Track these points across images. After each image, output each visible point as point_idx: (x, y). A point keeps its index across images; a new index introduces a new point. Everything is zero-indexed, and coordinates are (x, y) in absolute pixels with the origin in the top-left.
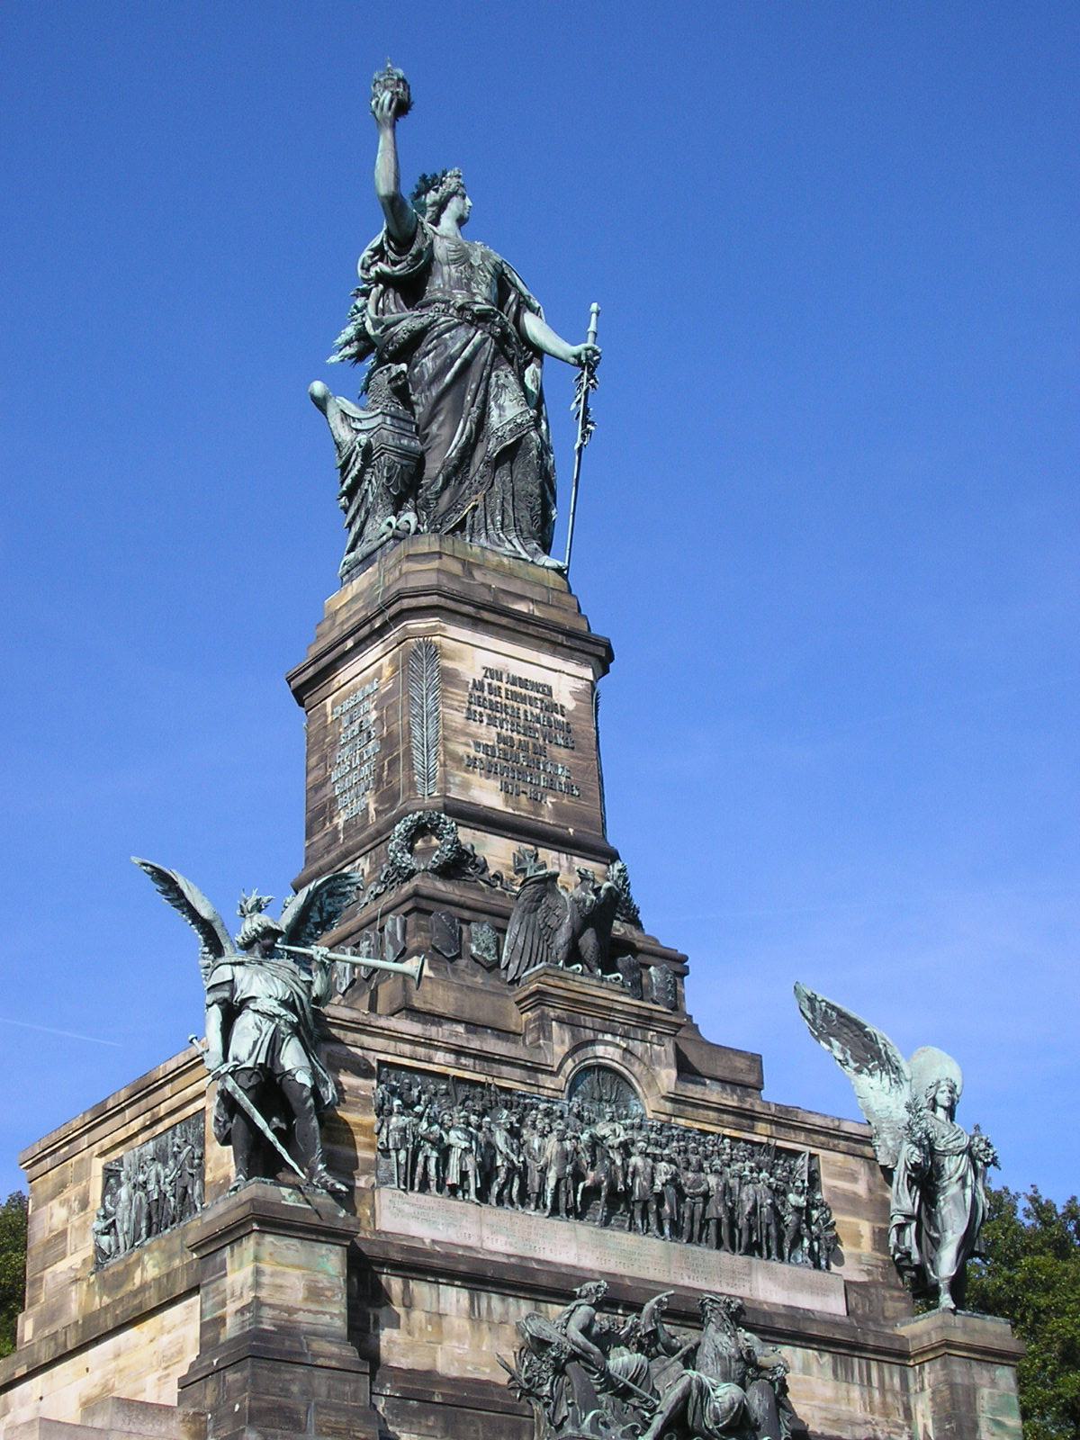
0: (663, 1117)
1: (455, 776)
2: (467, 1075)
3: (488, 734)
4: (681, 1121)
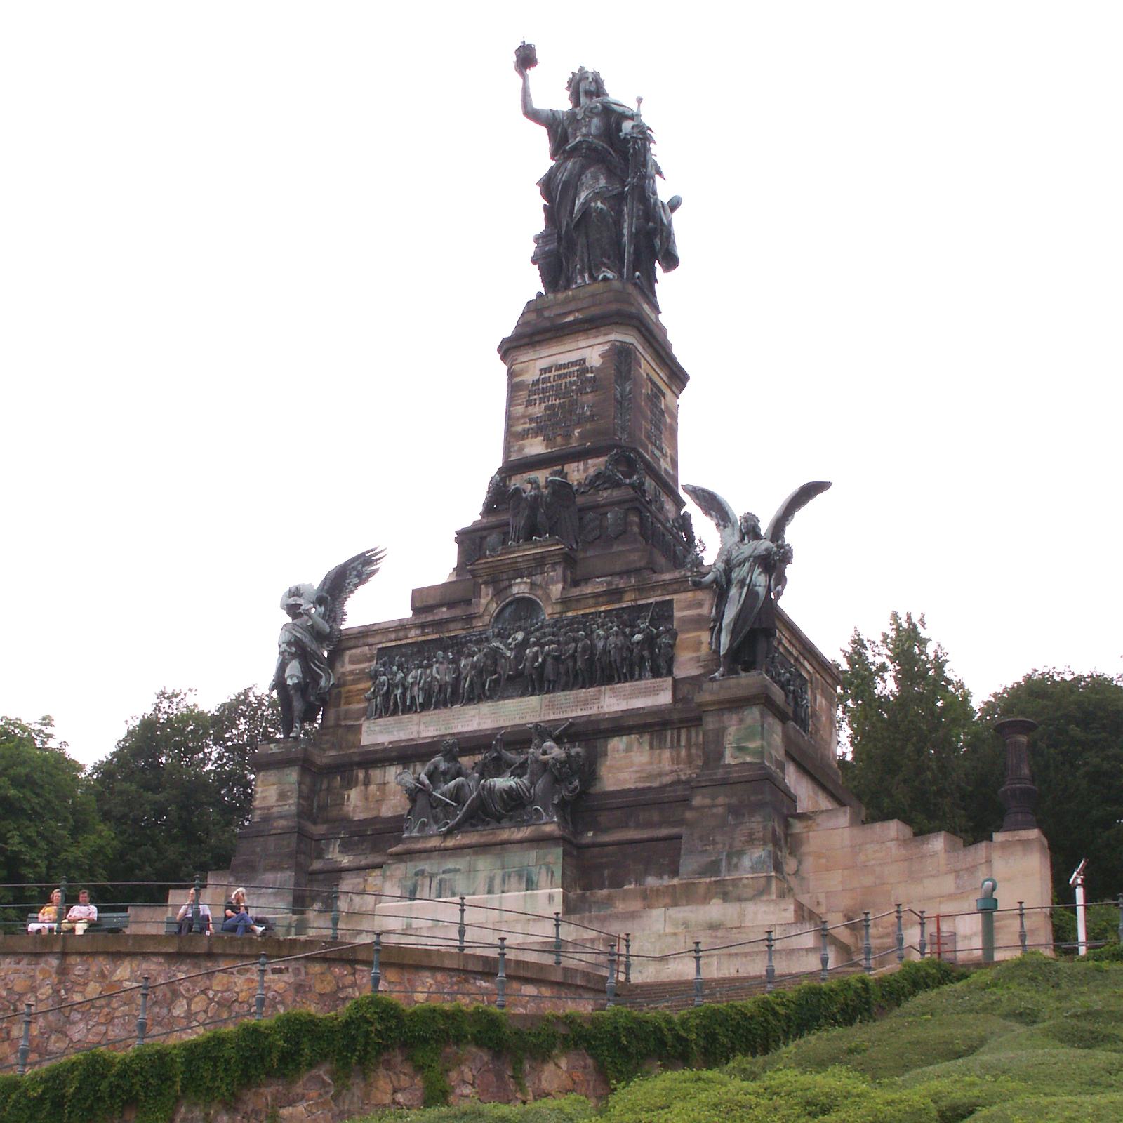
0: (557, 616)
1: (513, 446)
2: (430, 637)
3: (537, 410)
4: (570, 614)
